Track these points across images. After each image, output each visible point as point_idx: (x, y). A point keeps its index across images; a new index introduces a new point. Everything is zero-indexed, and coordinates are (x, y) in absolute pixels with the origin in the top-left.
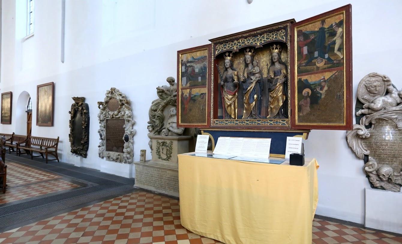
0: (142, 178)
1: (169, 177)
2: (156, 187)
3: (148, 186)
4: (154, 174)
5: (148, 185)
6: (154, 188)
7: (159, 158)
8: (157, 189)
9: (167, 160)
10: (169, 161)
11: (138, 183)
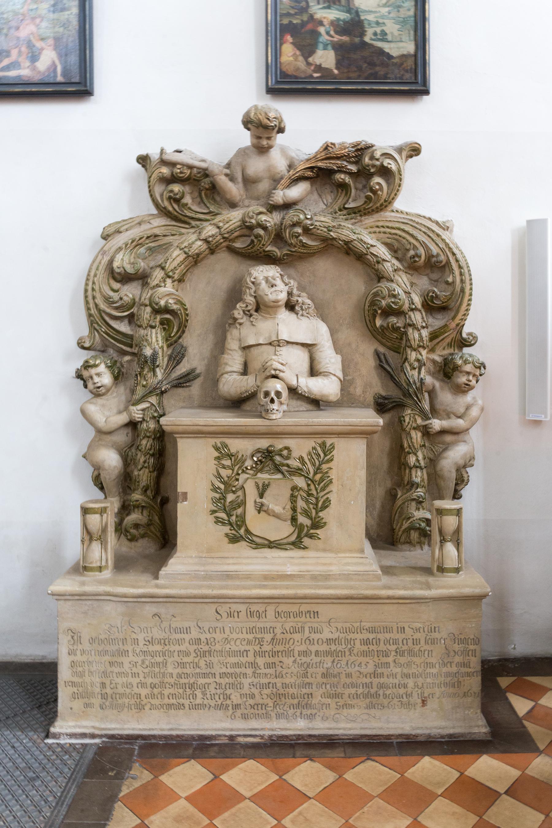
0: (119, 674)
1: (335, 636)
2: (237, 707)
3: (172, 712)
4: (218, 636)
6: (220, 713)
7: (234, 539)
8: (245, 717)
9: (293, 544)
10: (305, 548)
11: (87, 705)
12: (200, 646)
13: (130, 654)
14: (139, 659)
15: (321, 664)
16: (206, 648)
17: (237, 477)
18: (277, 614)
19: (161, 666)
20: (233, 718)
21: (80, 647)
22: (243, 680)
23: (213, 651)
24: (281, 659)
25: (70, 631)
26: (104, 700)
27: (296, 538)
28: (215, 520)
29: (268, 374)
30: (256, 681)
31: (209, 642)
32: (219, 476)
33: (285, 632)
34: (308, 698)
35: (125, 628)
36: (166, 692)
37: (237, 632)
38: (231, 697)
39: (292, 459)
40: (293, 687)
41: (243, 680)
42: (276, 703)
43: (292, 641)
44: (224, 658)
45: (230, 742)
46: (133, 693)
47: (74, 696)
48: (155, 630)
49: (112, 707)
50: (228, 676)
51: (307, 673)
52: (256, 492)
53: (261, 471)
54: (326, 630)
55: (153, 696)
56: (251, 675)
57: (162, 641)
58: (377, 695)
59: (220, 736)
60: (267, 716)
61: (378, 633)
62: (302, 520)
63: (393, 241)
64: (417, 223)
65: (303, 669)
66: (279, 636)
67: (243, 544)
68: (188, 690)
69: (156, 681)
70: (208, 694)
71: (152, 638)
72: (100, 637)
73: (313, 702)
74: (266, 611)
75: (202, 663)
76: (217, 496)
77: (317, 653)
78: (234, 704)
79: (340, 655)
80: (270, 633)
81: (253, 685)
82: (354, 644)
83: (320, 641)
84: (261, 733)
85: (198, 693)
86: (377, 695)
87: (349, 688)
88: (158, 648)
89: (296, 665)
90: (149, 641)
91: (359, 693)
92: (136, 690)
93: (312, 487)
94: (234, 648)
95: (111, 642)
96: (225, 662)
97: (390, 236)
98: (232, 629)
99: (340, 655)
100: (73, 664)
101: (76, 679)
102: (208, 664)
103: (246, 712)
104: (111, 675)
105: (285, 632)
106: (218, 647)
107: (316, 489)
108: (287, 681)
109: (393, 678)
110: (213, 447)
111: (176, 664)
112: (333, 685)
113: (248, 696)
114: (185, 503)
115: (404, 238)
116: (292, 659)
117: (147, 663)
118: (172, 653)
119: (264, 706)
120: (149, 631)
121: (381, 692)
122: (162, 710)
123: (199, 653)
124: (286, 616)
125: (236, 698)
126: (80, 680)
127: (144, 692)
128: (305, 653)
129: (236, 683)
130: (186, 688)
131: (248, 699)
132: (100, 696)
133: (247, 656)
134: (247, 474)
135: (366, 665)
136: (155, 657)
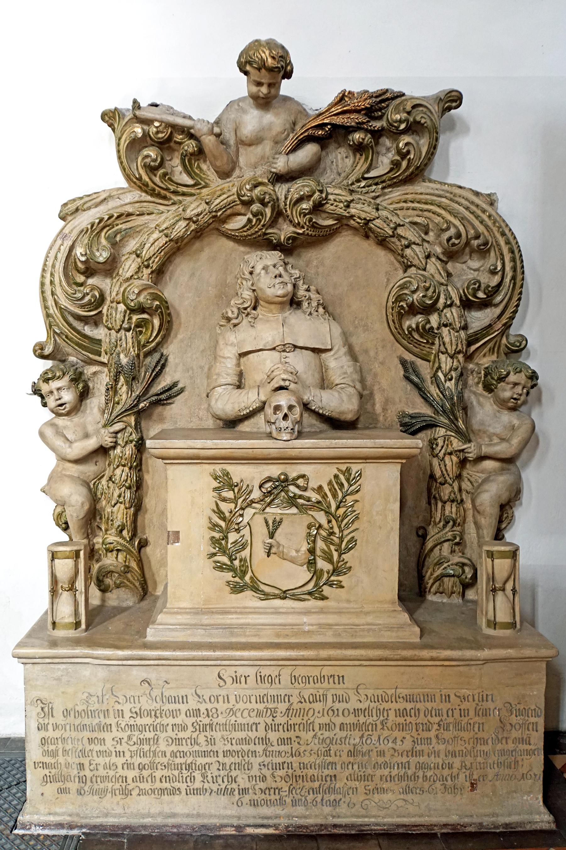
0: (100, 753)
2: (244, 791)
3: (166, 798)
4: (222, 706)
5: (162, 791)
6: (224, 800)
8: (254, 804)
12: (199, 719)
13: (114, 728)
14: (125, 735)
15: (347, 740)
16: (207, 721)
17: (241, 512)
18: (293, 678)
19: (152, 742)
20: (240, 804)
21: (52, 721)
22: (252, 760)
23: (215, 724)
24: (298, 733)
25: (39, 702)
26: (83, 785)
27: (314, 587)
28: (214, 565)
29: (277, 386)
30: (268, 760)
31: (210, 714)
32: (219, 512)
33: (303, 700)
34: (331, 780)
35: (107, 697)
36: (158, 774)
37: (245, 701)
38: (237, 780)
39: (309, 489)
40: (313, 767)
41: (252, 760)
42: (292, 787)
43: (311, 712)
44: (228, 733)
45: (237, 833)
46: (118, 776)
47: (46, 780)
48: (143, 699)
49: (93, 792)
50: (234, 754)
51: (330, 750)
52: (265, 531)
53: (269, 504)
54: (354, 698)
55: (142, 779)
56: (261, 753)
57: (153, 713)
58: (415, 777)
59: (226, 826)
60: (281, 802)
61: (417, 702)
62: (321, 564)
63: (423, 219)
64: (455, 195)
65: (324, 745)
66: (296, 706)
67: (249, 593)
68: (184, 771)
69: (145, 761)
70: (210, 776)
71: (140, 709)
72: (77, 708)
73: (337, 786)
74: (279, 675)
75: (202, 739)
76: (217, 535)
77: (342, 727)
78: (240, 787)
79: (370, 728)
80: (285, 702)
81: (264, 765)
82: (388, 716)
83: (346, 712)
84: (276, 821)
85: (197, 775)
86: (415, 777)
87: (381, 768)
88: (147, 721)
89: (316, 741)
90: (136, 713)
91: (393, 774)
92: (120, 772)
93: (334, 522)
94: (240, 720)
95: (90, 714)
96: (229, 737)
97: (420, 213)
98: (238, 697)
99: (370, 728)
100: (44, 741)
101: (47, 760)
102: (209, 740)
103: (256, 797)
104: (90, 754)
105: (303, 700)
106: (221, 720)
107: (339, 527)
108: (306, 760)
109: (435, 757)
110: (212, 476)
111: (170, 741)
112: (361, 766)
113: (258, 778)
114: (177, 544)
115: (439, 215)
116: (311, 734)
117: (134, 739)
118: (164, 727)
119: (277, 791)
120: (137, 701)
121: (421, 774)
122: (153, 795)
123: (198, 727)
124: (304, 681)
125: (243, 782)
126: (53, 761)
127: (131, 774)
128: (327, 727)
129: (243, 763)
130: (182, 769)
131: (258, 782)
132: (77, 780)
133: (257, 730)
134: (254, 508)
135: (402, 741)
136: (144, 732)
